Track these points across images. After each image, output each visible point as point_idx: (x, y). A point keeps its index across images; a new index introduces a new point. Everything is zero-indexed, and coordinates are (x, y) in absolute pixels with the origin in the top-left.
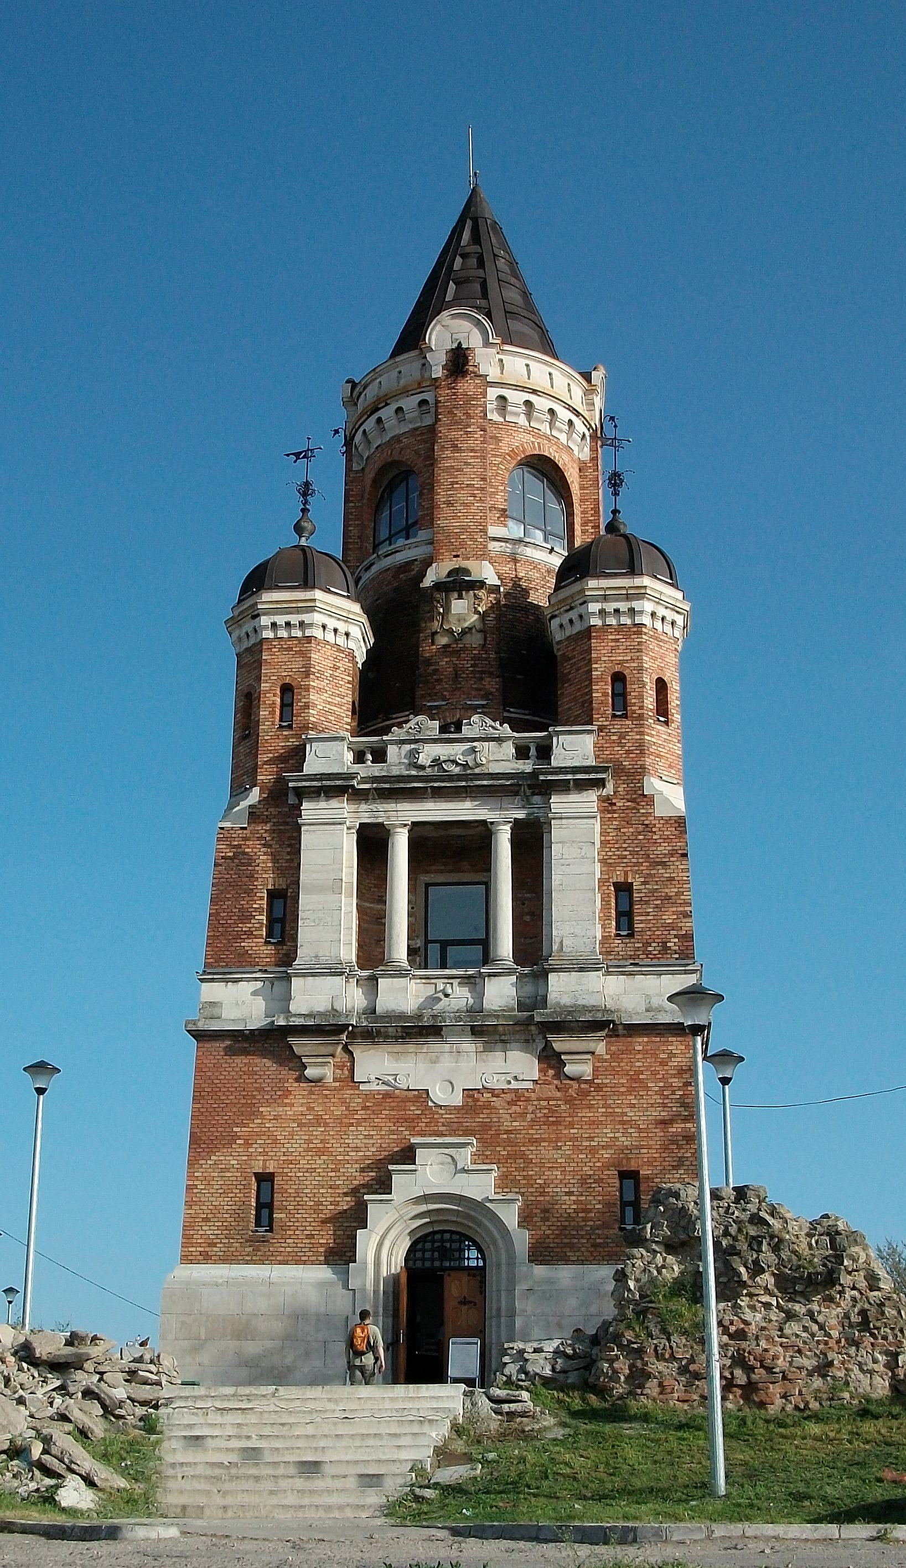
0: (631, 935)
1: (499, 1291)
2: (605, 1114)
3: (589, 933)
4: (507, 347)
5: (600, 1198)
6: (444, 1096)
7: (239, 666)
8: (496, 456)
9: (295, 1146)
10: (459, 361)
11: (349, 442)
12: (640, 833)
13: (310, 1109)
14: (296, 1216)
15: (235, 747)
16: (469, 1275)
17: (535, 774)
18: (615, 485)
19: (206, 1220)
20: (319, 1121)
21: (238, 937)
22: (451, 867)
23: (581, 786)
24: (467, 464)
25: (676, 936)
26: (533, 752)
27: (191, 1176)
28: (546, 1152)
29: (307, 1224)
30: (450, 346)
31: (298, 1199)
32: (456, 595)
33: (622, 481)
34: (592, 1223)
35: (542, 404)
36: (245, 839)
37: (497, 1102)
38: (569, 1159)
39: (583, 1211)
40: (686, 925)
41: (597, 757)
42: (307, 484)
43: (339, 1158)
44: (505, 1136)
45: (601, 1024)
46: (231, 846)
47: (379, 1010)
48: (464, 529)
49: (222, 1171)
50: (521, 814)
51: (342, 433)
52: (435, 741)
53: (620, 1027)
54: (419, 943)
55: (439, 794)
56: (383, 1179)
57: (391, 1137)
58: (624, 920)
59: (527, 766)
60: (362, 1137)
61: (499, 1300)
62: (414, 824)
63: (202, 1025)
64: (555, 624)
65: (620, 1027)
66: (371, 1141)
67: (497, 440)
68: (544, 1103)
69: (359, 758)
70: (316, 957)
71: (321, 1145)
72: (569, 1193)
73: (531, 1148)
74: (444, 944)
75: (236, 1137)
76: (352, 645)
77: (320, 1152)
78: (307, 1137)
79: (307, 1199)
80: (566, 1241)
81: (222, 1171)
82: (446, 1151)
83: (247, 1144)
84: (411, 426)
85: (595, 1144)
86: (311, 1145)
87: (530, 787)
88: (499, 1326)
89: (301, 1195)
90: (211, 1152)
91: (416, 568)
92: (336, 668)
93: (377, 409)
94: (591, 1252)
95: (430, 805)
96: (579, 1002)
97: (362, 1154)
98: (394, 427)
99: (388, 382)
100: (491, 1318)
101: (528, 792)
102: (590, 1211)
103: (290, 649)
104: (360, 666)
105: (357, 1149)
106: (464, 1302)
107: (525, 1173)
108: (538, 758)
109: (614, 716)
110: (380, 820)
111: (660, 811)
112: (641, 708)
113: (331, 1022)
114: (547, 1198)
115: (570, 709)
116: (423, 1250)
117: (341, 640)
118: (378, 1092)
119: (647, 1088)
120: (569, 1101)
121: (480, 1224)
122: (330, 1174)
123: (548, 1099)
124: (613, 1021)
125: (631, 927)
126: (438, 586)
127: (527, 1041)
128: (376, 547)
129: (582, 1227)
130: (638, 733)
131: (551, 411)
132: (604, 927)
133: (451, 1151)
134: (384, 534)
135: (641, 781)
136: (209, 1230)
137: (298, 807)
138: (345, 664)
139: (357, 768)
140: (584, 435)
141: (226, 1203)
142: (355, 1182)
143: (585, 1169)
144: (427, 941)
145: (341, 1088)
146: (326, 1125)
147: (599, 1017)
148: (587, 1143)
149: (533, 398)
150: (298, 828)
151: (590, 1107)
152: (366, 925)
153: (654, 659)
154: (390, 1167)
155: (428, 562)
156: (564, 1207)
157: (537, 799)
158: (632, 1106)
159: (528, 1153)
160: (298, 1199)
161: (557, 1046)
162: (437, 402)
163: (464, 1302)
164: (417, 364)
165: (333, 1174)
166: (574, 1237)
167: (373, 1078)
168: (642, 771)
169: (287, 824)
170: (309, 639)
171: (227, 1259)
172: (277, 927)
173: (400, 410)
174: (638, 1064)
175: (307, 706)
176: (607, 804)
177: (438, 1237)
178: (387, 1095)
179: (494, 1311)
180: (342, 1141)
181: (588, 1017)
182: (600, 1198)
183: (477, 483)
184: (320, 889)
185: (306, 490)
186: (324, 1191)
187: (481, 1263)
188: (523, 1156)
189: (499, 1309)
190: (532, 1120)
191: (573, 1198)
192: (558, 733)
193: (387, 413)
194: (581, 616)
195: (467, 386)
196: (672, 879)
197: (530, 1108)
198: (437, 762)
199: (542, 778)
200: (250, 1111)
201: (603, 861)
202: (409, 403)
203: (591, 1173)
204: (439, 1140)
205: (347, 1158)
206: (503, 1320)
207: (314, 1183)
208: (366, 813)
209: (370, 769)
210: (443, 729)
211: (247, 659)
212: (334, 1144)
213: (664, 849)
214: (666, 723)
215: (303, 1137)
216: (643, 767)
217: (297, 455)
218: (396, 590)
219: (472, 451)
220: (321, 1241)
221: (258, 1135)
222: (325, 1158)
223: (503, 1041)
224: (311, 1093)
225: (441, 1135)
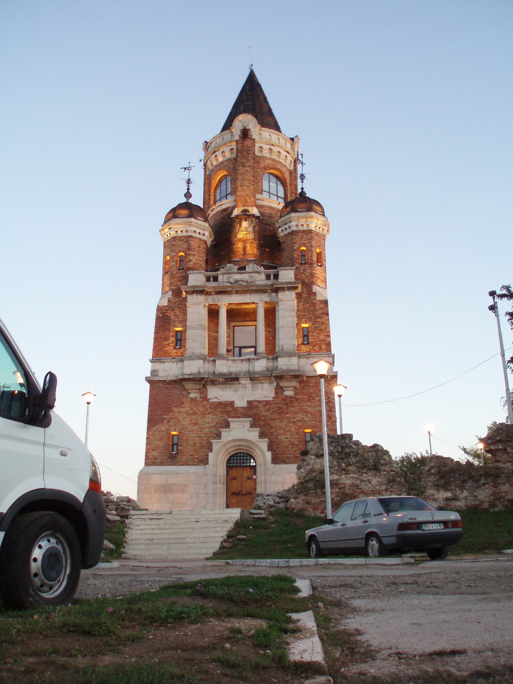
0: (308, 344)
1: (261, 474)
2: (300, 409)
3: (293, 343)
4: (262, 128)
6: (241, 403)
7: (164, 247)
8: (258, 169)
9: (186, 422)
10: (245, 133)
11: (205, 165)
12: (311, 306)
13: (192, 409)
15: (163, 276)
17: (272, 285)
18: (302, 179)
19: (154, 450)
20: (194, 413)
21: (164, 346)
22: (242, 320)
23: (289, 289)
24: (248, 171)
25: (325, 344)
26: (272, 277)
27: (148, 434)
28: (277, 423)
30: (241, 128)
32: (244, 220)
33: (305, 177)
34: (294, 449)
35: (275, 149)
36: (167, 310)
37: (260, 405)
38: (286, 426)
40: (328, 339)
41: (295, 279)
42: (189, 180)
45: (297, 376)
46: (162, 313)
47: (216, 372)
48: (247, 196)
49: (160, 432)
50: (267, 300)
51: (203, 160)
52: (236, 273)
53: (304, 377)
54: (231, 348)
55: (237, 292)
58: (306, 338)
59: (269, 282)
61: (261, 477)
62: (229, 304)
63: (151, 379)
64: (280, 230)
65: (304, 377)
67: (258, 162)
68: (277, 405)
69: (208, 279)
70: (193, 353)
72: (286, 438)
74: (241, 348)
75: (164, 419)
76: (205, 238)
80: (285, 455)
81: (160, 432)
83: (168, 422)
84: (227, 158)
87: (271, 290)
88: (261, 487)
90: (155, 425)
91: (229, 210)
92: (199, 247)
93: (215, 152)
95: (234, 296)
96: (290, 368)
98: (221, 159)
99: (219, 141)
101: (270, 291)
103: (183, 240)
104: (209, 246)
105: (208, 423)
108: (274, 279)
109: (302, 264)
110: (216, 303)
111: (319, 298)
112: (312, 260)
113: (199, 377)
115: (285, 261)
116: (234, 460)
117: (201, 237)
118: (216, 402)
119: (314, 399)
120: (286, 404)
121: (254, 450)
123: (279, 404)
124: (301, 375)
125: (308, 341)
126: (237, 217)
127: (270, 383)
128: (215, 202)
130: (311, 270)
131: (279, 152)
132: (298, 341)
133: (243, 423)
134: (218, 198)
135: (312, 287)
136: (155, 454)
137: (185, 298)
138: (203, 246)
139: (207, 283)
140: (291, 161)
141: (161, 444)
144: (234, 347)
145: (202, 401)
146: (197, 414)
147: (297, 373)
149: (272, 147)
150: (186, 306)
151: (294, 406)
152: (212, 341)
153: (316, 242)
154: (221, 430)
155: (234, 208)
157: (273, 294)
158: (309, 406)
161: (282, 384)
162: (237, 149)
164: (230, 135)
166: (288, 454)
167: (214, 397)
168: (313, 283)
169: (182, 304)
170: (190, 237)
171: (162, 464)
172: (179, 342)
173: (223, 152)
174: (311, 391)
175: (189, 261)
176: (299, 296)
177: (239, 455)
178: (220, 403)
179: (259, 482)
181: (293, 374)
183: (252, 179)
184: (194, 328)
185: (189, 182)
187: (254, 464)
188: (269, 424)
189: (261, 481)
190: (273, 412)
192: (281, 270)
193: (219, 153)
194: (289, 227)
195: (248, 142)
196: (323, 323)
197: (272, 408)
198: (237, 281)
199: (275, 286)
200: (169, 410)
201: (298, 317)
202: (227, 150)
204: (238, 419)
208: (211, 300)
209: (212, 284)
210: (239, 269)
211: (168, 244)
212: (200, 421)
213: (320, 312)
214: (321, 266)
216: (312, 282)
217: (185, 168)
218: (222, 218)
219: (250, 166)
221: (172, 418)
223: (262, 383)
224: (192, 403)
225: (239, 417)
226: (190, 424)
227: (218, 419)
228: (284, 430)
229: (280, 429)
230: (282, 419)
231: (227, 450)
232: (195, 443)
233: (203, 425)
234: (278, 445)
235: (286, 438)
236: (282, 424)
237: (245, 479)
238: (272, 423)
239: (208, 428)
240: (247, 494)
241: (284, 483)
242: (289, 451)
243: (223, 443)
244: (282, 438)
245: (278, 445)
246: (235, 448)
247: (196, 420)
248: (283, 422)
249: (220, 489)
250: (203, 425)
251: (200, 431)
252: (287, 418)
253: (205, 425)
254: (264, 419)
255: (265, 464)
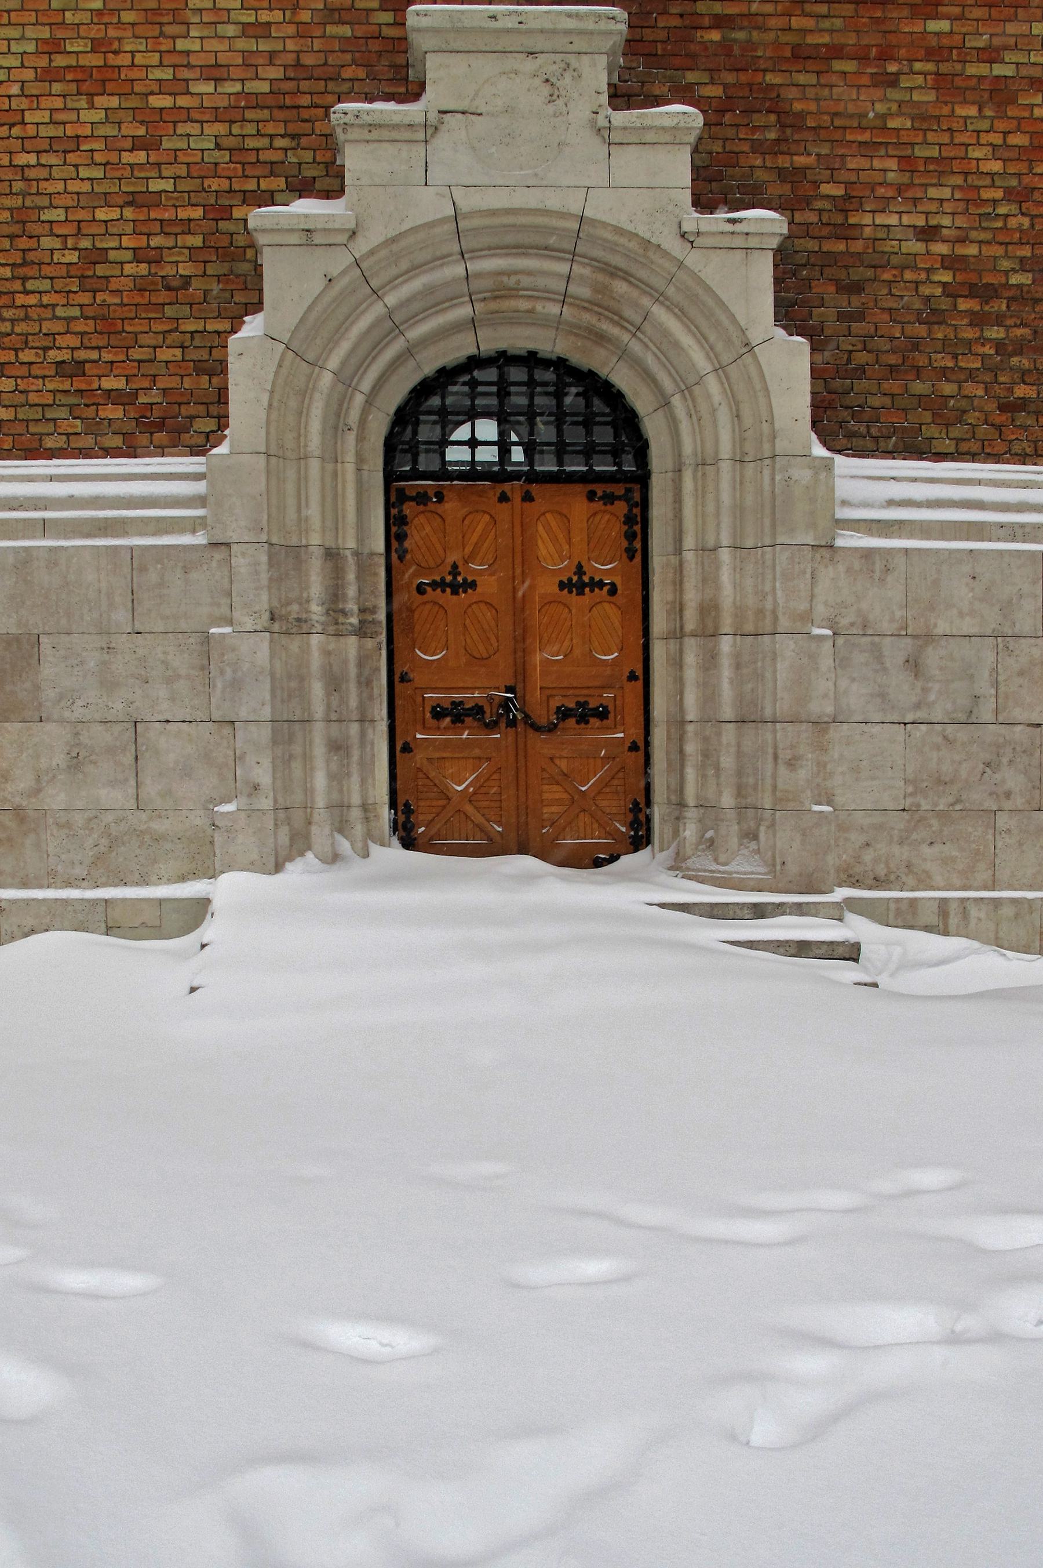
5: (1026, 252)
14: (20, 300)
16: (591, 496)
29: (59, 327)
31: (23, 243)
34: (995, 333)
38: (923, 120)
39: (973, 291)
43: (158, 102)
44: (715, 36)
56: (309, 172)
57: (331, 30)
60: (231, 30)
61: (709, 579)
66: (264, 46)
71: (96, 60)
73: (802, 78)
77: (93, 82)
78: (45, 33)
79: (57, 243)
80: (919, 387)
82: (529, 65)
85: (1008, 71)
86: (60, 61)
89: (34, 229)
94: (999, 428)
97: (237, 87)
100: (678, 634)
102: (987, 293)
106: (578, 584)
107: (783, 161)
114: (857, 246)
122: (127, 158)
129: (969, 343)
142: (215, 184)
143: (975, 153)
148: (983, 69)
156: (908, 275)
159: (792, 93)
160: (23, 243)
163: (578, 584)
165: (141, 157)
180: (166, 45)
182: (1026, 252)
186: (114, 214)
189: (709, 609)
191: (942, 248)
203: (996, 166)
205: (183, 101)
206: (726, 644)
207: (74, 186)
215: (30, 32)
220: (108, 383)
222: (114, 102)
226: (49, 75)
227: (303, 32)
228: (907, 163)
229: (868, 148)
230: (886, 55)
231: (393, 325)
232: (96, 256)
233: (162, 88)
234: (856, 288)
235: (928, 233)
236: (876, 105)
237: (548, 587)
238: (800, 90)
239: (217, 115)
240: (564, 713)
241: (928, 638)
242: (955, 347)
243: (362, 246)
244: (892, 223)
245: (856, 288)
246: (464, 311)
247: (97, 45)
248: (892, 81)
249: (334, 684)
250: (162, 88)
251: (138, 144)
252: (933, 54)
253: (179, 87)
254: (726, 47)
255: (757, 451)
